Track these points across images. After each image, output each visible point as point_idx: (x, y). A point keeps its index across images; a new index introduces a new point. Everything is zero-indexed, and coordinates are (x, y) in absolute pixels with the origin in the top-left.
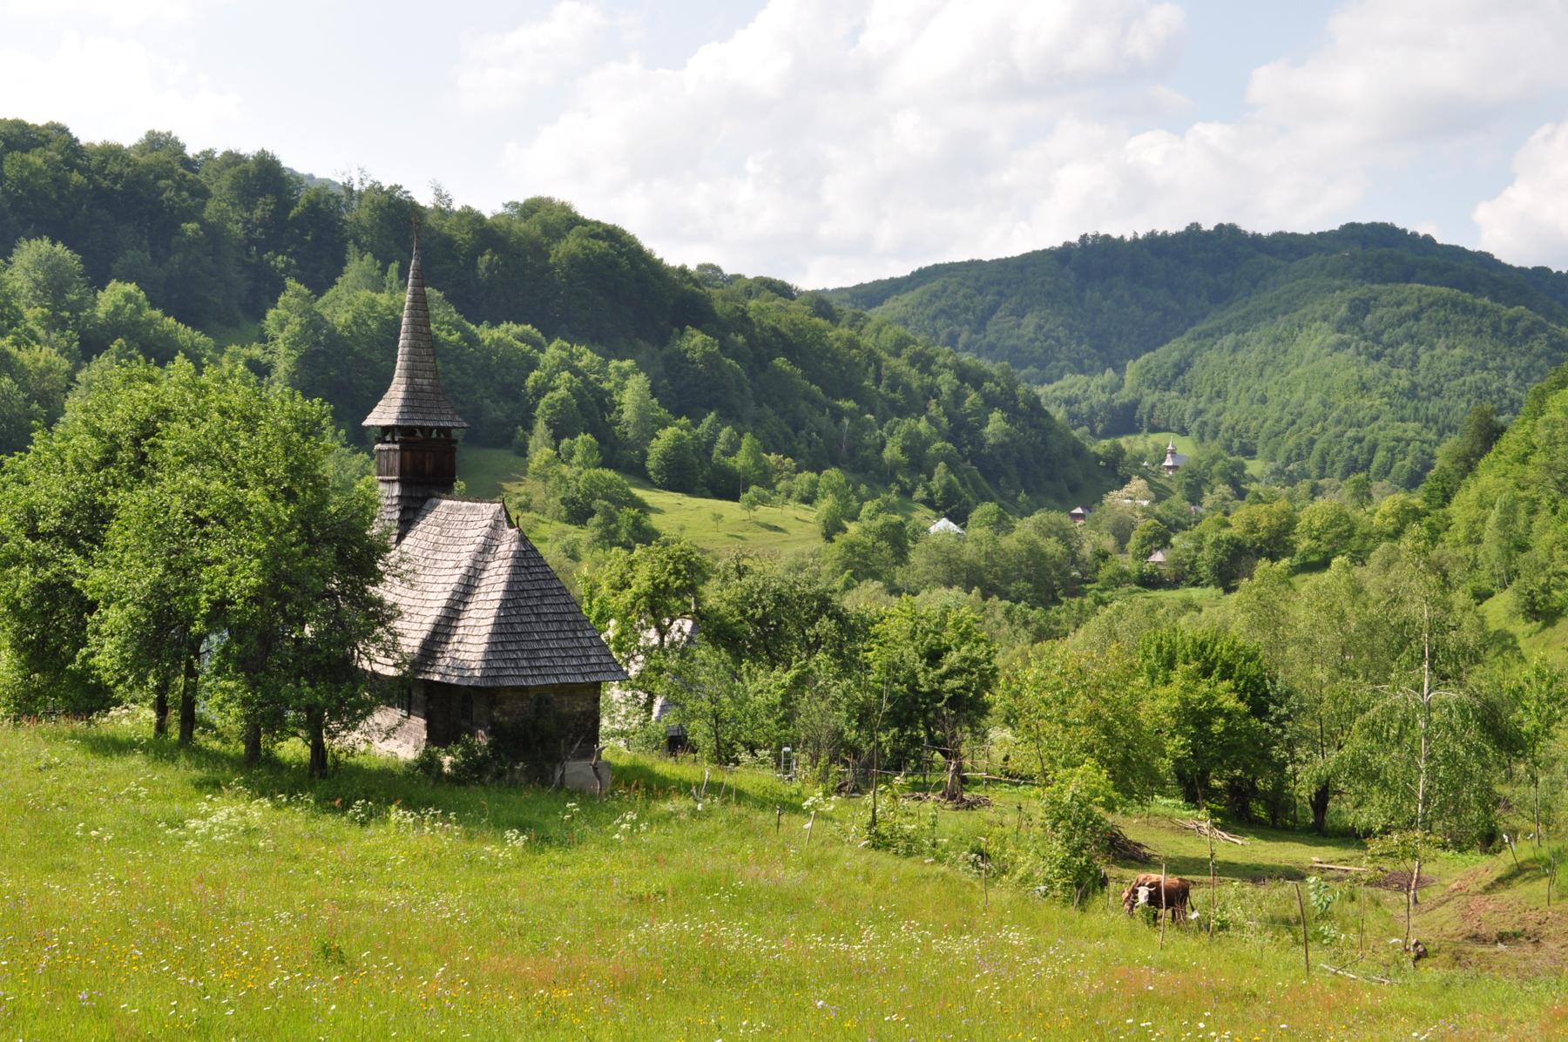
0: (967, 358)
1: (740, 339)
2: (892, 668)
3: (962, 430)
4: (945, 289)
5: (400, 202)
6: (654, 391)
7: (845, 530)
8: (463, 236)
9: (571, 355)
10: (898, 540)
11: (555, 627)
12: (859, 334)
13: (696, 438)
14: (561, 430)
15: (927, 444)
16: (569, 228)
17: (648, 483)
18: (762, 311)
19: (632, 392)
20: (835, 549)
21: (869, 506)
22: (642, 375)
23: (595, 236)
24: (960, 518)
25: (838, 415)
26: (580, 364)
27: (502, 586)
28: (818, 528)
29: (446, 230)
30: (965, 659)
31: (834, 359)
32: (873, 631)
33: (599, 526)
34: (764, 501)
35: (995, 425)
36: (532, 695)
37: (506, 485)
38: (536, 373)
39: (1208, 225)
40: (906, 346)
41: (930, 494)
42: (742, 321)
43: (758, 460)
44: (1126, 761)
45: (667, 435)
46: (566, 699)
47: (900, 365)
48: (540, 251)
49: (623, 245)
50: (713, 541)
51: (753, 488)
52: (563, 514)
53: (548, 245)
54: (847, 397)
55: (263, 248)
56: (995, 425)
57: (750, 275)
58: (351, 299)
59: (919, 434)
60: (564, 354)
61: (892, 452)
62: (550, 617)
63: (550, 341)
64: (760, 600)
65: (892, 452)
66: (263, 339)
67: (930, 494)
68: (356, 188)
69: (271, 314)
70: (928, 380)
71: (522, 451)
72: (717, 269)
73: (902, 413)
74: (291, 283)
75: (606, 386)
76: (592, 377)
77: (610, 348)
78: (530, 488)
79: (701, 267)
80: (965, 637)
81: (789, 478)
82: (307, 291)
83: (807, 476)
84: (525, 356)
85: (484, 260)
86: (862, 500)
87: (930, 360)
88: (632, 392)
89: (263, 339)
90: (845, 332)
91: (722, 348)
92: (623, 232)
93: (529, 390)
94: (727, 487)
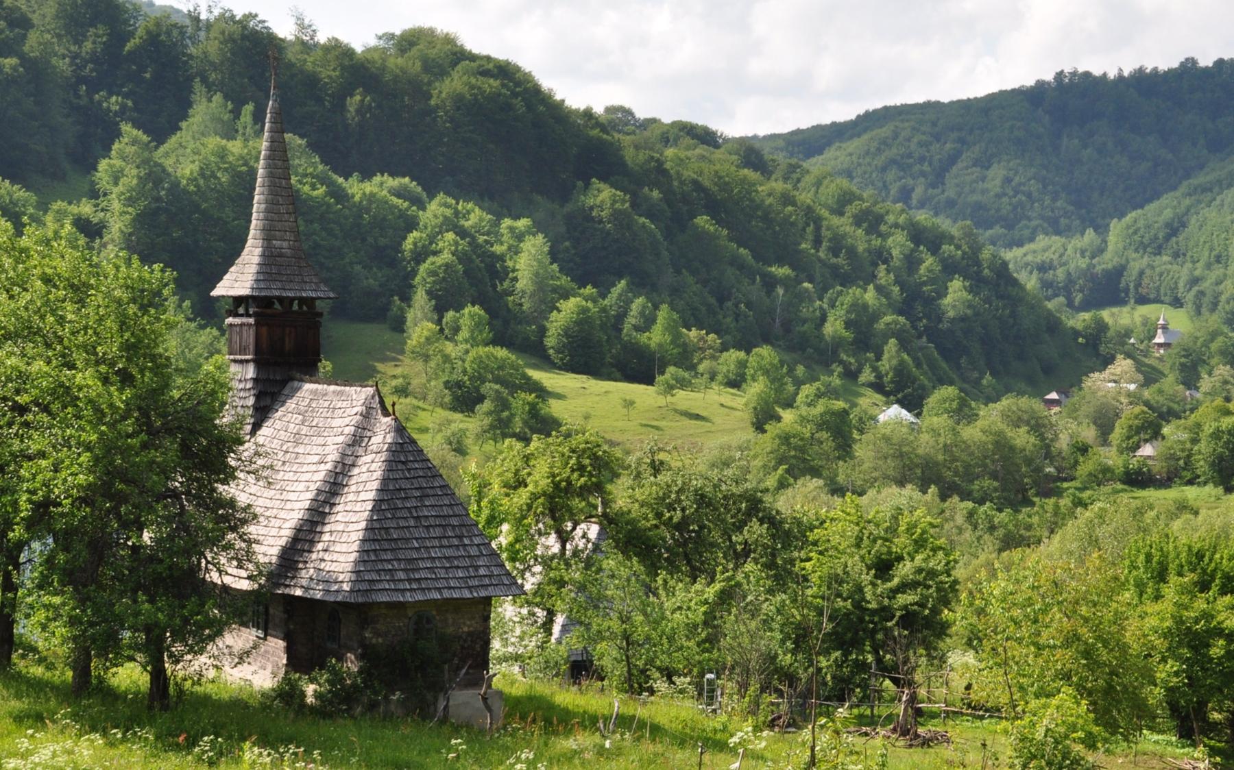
0: (922, 217)
1: (656, 194)
2: (835, 580)
3: (916, 301)
4: (896, 136)
5: (255, 33)
6: (554, 255)
7: (779, 419)
8: (329, 73)
9: (457, 213)
10: (841, 431)
11: (437, 532)
12: (796, 188)
13: (604, 310)
14: (443, 302)
15: (875, 317)
16: (454, 64)
17: (548, 364)
18: (681, 161)
19: (528, 257)
20: (767, 441)
21: (807, 390)
22: (540, 236)
23: (485, 73)
24: (913, 404)
25: (770, 283)
26: (467, 224)
27: (376, 485)
28: (747, 416)
29: (309, 66)
30: (919, 571)
31: (767, 218)
32: (811, 537)
33: (488, 414)
34: (683, 384)
35: (956, 294)
36: (410, 613)
37: (380, 366)
38: (415, 234)
39: (1206, 61)
40: (850, 202)
41: (879, 376)
42: (658, 173)
43: (677, 336)
44: (1109, 690)
45: (569, 308)
47: (843, 224)
48: (419, 91)
49: (518, 84)
50: (623, 431)
51: (671, 369)
52: (447, 399)
53: (430, 83)
54: (781, 262)
55: (94, 87)
56: (956, 294)
57: (667, 119)
58: (199, 147)
59: (865, 306)
60: (448, 212)
61: (834, 327)
62: (432, 521)
63: (431, 196)
64: (679, 501)
65: (834, 327)
66: (94, 194)
67: (879, 376)
68: (203, 17)
69: (103, 165)
70: (877, 242)
71: (399, 326)
72: (628, 112)
73: (847, 281)
74: (126, 128)
75: (498, 249)
76: (481, 239)
77: (501, 202)
78: (408, 369)
79: (609, 110)
80: (920, 544)
81: (713, 358)
82: (145, 138)
83: (734, 355)
84: (402, 214)
85: (354, 101)
86: (799, 383)
87: (880, 219)
88: (528, 257)
89: (94, 194)
90: (778, 186)
91: (634, 205)
92: (518, 69)
93: (407, 255)
94: (639, 368)
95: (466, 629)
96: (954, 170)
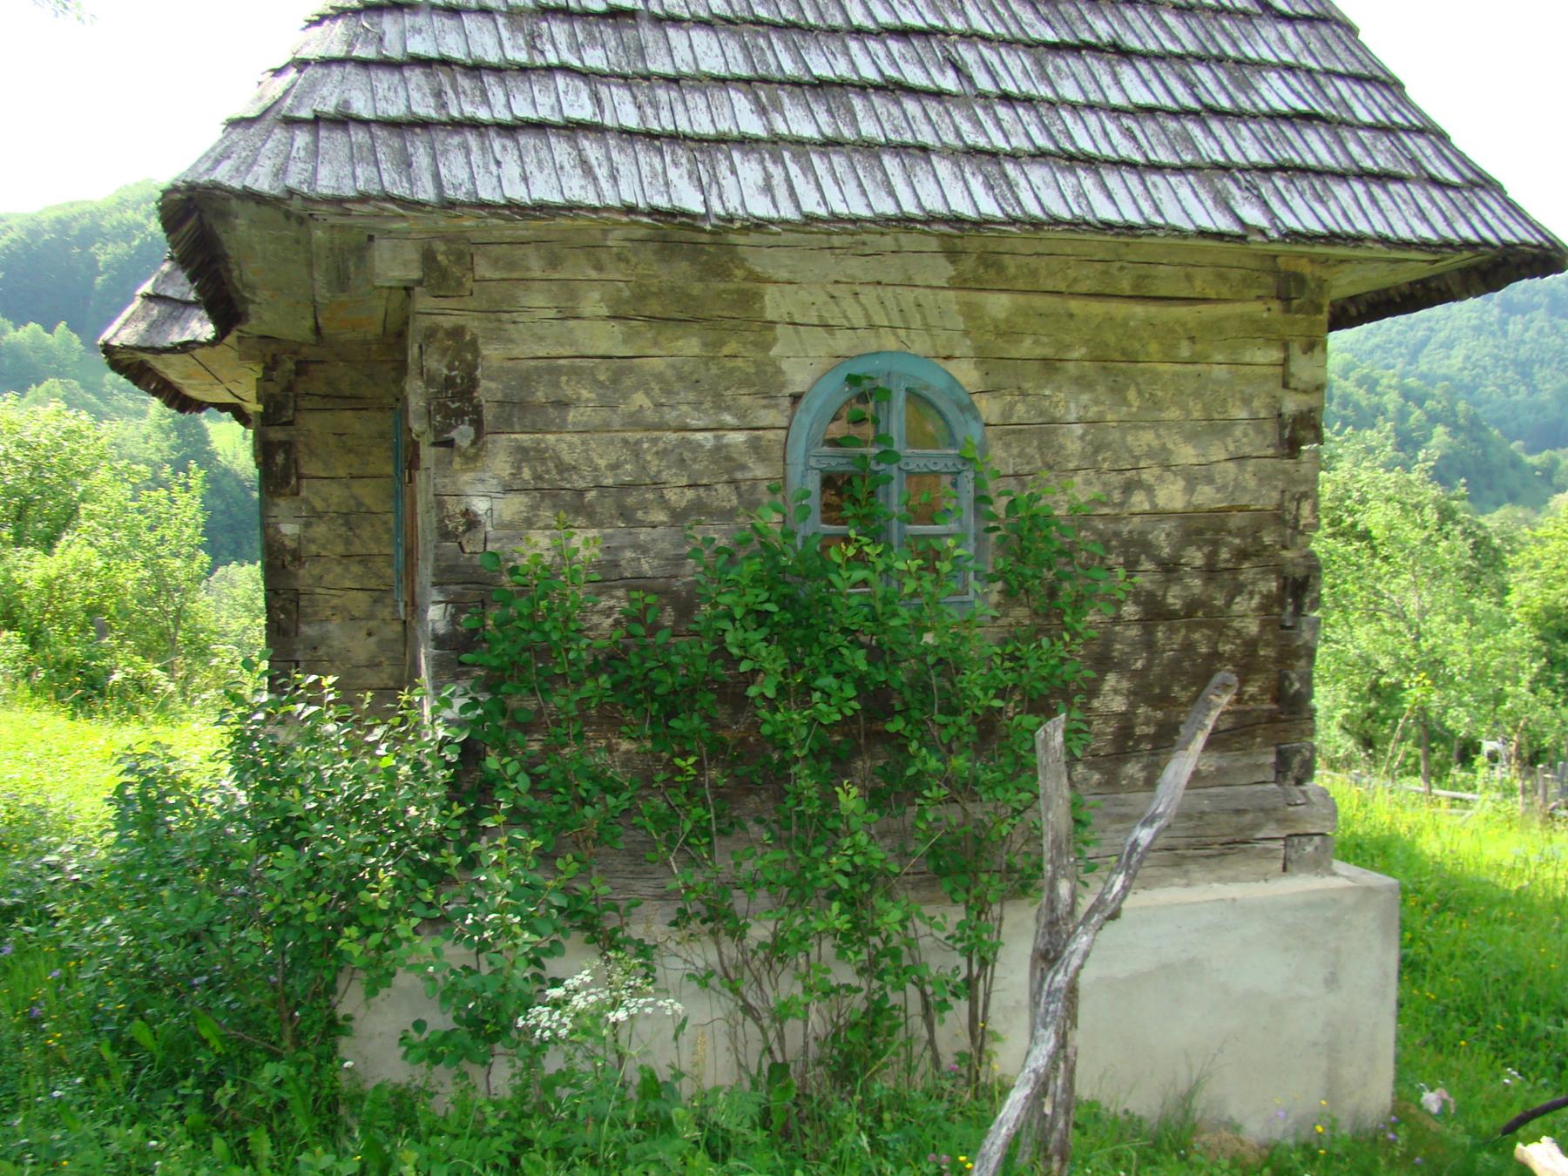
46: (1070, 405)
70: (1375, 399)
87: (1376, 382)
95: (1171, 495)
96: (1426, 351)
